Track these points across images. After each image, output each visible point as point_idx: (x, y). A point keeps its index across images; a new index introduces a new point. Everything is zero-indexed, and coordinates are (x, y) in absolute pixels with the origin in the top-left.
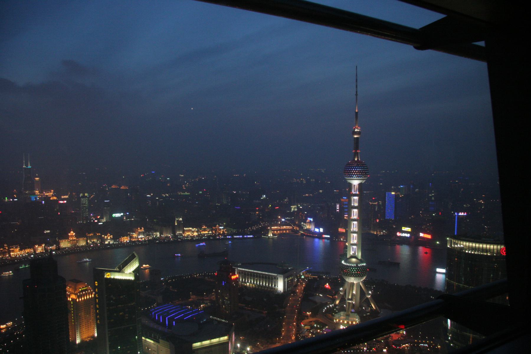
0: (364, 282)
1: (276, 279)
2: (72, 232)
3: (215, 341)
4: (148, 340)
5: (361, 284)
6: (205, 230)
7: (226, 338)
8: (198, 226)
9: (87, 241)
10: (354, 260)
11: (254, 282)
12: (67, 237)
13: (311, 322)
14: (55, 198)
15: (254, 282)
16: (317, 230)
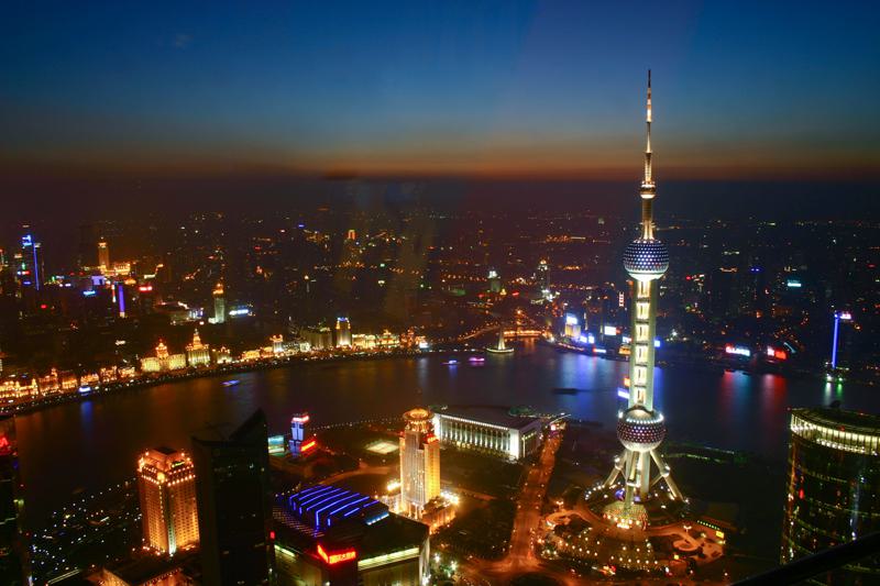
0: (658, 451)
1: (506, 435)
2: (161, 345)
3: (397, 556)
4: (284, 551)
5: (652, 454)
6: (388, 338)
7: (412, 552)
8: (378, 331)
9: (187, 359)
10: (639, 413)
11: (469, 439)
12: (153, 354)
13: (564, 517)
14: (133, 282)
15: (469, 439)
16: (583, 339)
